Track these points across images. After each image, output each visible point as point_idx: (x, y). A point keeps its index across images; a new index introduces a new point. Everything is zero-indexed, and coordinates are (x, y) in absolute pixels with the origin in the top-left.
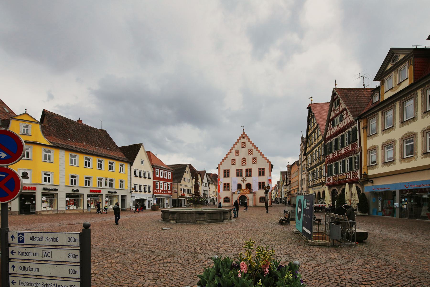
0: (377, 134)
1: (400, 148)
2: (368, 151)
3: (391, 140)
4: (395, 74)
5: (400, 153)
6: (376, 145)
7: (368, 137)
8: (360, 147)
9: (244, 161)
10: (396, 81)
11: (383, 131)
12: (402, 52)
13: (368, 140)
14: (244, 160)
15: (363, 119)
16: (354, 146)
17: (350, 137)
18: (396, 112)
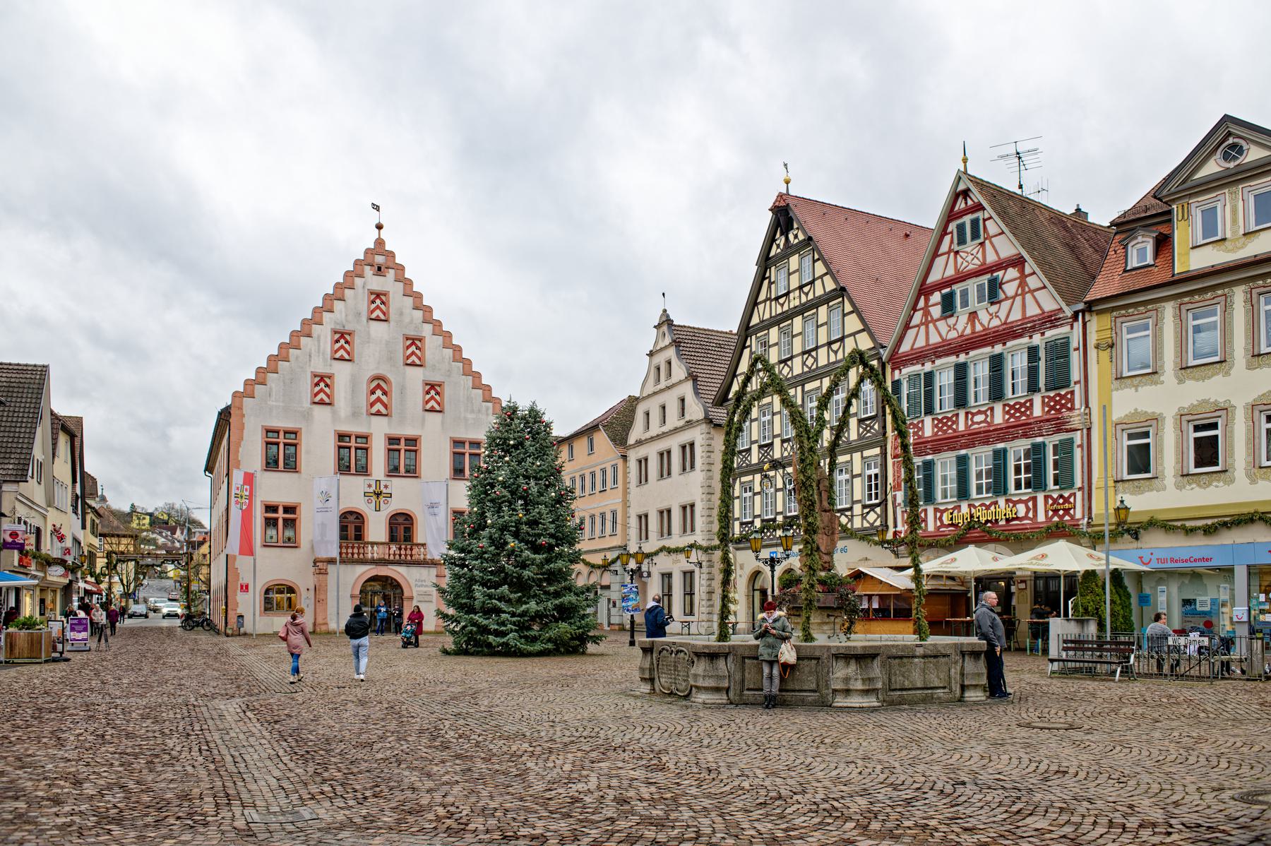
0: (1156, 376)
1: (1247, 434)
2: (1119, 427)
3: (1216, 403)
4: (1234, 200)
5: (1248, 449)
6: (1153, 413)
7: (1116, 379)
8: (1087, 411)
9: (379, 393)
10: (1234, 221)
11: (1181, 369)
12: (1262, 142)
13: (1117, 389)
14: (379, 386)
15: (1097, 314)
16: (1060, 405)
17: (1037, 368)
18: (1232, 317)
